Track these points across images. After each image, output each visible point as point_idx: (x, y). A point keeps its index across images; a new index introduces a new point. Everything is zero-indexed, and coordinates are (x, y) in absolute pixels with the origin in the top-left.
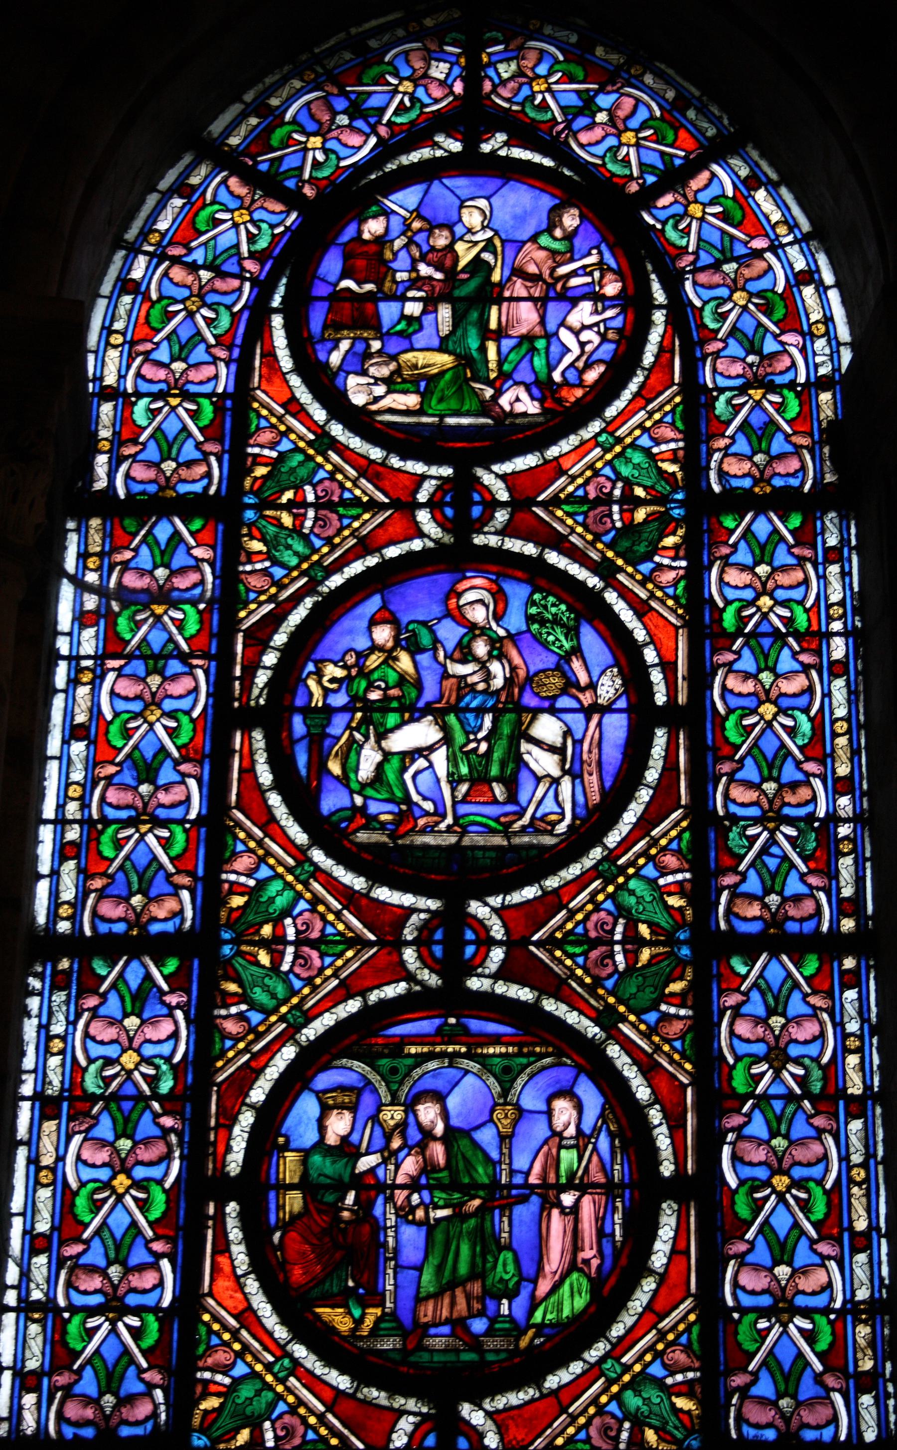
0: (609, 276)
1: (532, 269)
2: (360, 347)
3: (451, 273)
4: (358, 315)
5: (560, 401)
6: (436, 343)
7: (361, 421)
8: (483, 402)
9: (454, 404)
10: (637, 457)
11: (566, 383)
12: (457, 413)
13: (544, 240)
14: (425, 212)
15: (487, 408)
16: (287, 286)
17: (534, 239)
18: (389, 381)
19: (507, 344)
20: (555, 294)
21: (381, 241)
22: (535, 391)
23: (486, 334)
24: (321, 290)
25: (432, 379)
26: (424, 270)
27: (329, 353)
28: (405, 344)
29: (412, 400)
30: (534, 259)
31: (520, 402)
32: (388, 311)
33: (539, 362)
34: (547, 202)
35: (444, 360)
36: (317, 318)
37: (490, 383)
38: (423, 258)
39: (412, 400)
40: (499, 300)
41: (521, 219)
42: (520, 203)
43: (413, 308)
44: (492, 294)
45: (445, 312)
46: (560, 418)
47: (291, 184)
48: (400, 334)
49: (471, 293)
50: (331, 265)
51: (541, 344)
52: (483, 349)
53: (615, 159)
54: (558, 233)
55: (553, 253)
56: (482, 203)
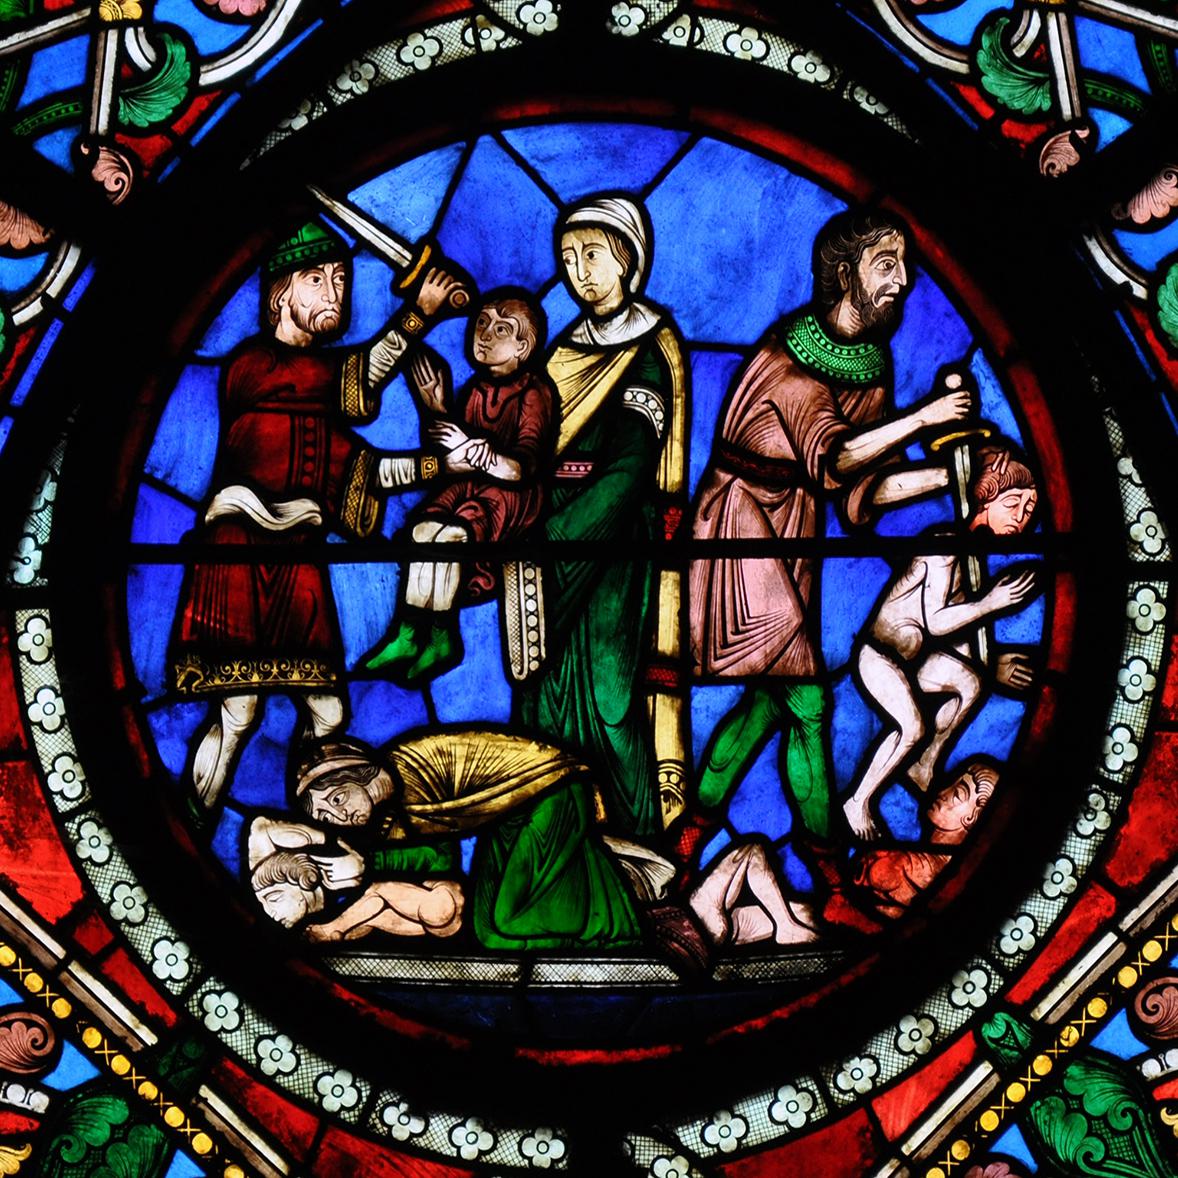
0: (1001, 467)
1: (774, 443)
2: (280, 720)
3: (538, 456)
4: (266, 609)
5: (868, 899)
6: (500, 702)
7: (288, 975)
8: (643, 905)
9: (559, 916)
10: (1100, 1095)
11: (883, 836)
12: (572, 949)
13: (806, 342)
14: (460, 248)
15: (659, 925)
16: (58, 506)
17: (776, 337)
18: (363, 838)
19: (710, 702)
20: (846, 533)
21: (333, 346)
22: (794, 866)
23: (650, 673)
24: (162, 525)
25: (499, 828)
26: (461, 448)
27: (193, 745)
28: (411, 711)
29: (435, 904)
30: (780, 408)
31: (751, 903)
32: (359, 593)
33: (804, 766)
34: (810, 208)
35: (525, 759)
36: (151, 622)
37: (663, 842)
38: (456, 411)
39: (435, 904)
40: (682, 553)
41: (735, 269)
42: (731, 209)
43: (432, 584)
44: (658, 536)
45: (525, 595)
46: (876, 962)
47: (55, 148)
48: (397, 673)
49: (595, 529)
50: (187, 435)
51: (806, 703)
52: (640, 725)
53: (1008, 63)
54: (846, 317)
55: (835, 385)
56: (622, 213)
